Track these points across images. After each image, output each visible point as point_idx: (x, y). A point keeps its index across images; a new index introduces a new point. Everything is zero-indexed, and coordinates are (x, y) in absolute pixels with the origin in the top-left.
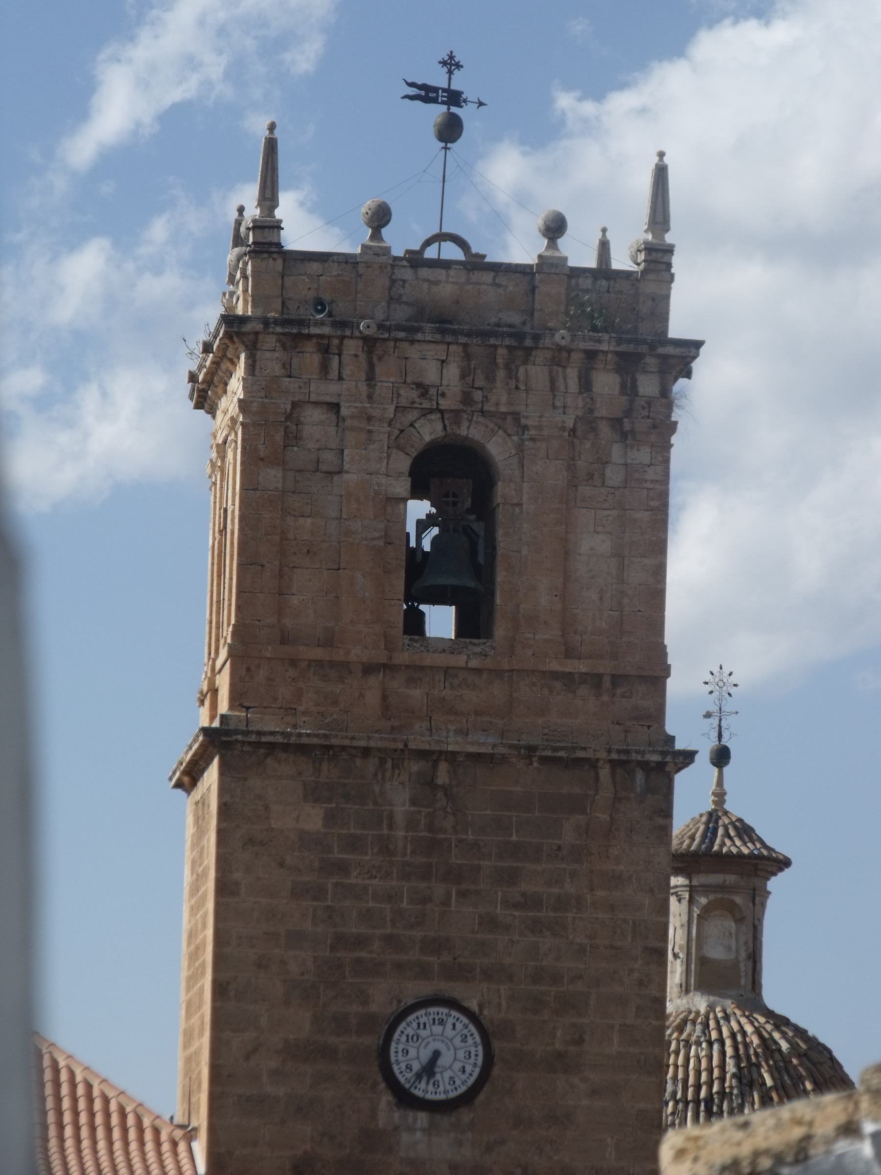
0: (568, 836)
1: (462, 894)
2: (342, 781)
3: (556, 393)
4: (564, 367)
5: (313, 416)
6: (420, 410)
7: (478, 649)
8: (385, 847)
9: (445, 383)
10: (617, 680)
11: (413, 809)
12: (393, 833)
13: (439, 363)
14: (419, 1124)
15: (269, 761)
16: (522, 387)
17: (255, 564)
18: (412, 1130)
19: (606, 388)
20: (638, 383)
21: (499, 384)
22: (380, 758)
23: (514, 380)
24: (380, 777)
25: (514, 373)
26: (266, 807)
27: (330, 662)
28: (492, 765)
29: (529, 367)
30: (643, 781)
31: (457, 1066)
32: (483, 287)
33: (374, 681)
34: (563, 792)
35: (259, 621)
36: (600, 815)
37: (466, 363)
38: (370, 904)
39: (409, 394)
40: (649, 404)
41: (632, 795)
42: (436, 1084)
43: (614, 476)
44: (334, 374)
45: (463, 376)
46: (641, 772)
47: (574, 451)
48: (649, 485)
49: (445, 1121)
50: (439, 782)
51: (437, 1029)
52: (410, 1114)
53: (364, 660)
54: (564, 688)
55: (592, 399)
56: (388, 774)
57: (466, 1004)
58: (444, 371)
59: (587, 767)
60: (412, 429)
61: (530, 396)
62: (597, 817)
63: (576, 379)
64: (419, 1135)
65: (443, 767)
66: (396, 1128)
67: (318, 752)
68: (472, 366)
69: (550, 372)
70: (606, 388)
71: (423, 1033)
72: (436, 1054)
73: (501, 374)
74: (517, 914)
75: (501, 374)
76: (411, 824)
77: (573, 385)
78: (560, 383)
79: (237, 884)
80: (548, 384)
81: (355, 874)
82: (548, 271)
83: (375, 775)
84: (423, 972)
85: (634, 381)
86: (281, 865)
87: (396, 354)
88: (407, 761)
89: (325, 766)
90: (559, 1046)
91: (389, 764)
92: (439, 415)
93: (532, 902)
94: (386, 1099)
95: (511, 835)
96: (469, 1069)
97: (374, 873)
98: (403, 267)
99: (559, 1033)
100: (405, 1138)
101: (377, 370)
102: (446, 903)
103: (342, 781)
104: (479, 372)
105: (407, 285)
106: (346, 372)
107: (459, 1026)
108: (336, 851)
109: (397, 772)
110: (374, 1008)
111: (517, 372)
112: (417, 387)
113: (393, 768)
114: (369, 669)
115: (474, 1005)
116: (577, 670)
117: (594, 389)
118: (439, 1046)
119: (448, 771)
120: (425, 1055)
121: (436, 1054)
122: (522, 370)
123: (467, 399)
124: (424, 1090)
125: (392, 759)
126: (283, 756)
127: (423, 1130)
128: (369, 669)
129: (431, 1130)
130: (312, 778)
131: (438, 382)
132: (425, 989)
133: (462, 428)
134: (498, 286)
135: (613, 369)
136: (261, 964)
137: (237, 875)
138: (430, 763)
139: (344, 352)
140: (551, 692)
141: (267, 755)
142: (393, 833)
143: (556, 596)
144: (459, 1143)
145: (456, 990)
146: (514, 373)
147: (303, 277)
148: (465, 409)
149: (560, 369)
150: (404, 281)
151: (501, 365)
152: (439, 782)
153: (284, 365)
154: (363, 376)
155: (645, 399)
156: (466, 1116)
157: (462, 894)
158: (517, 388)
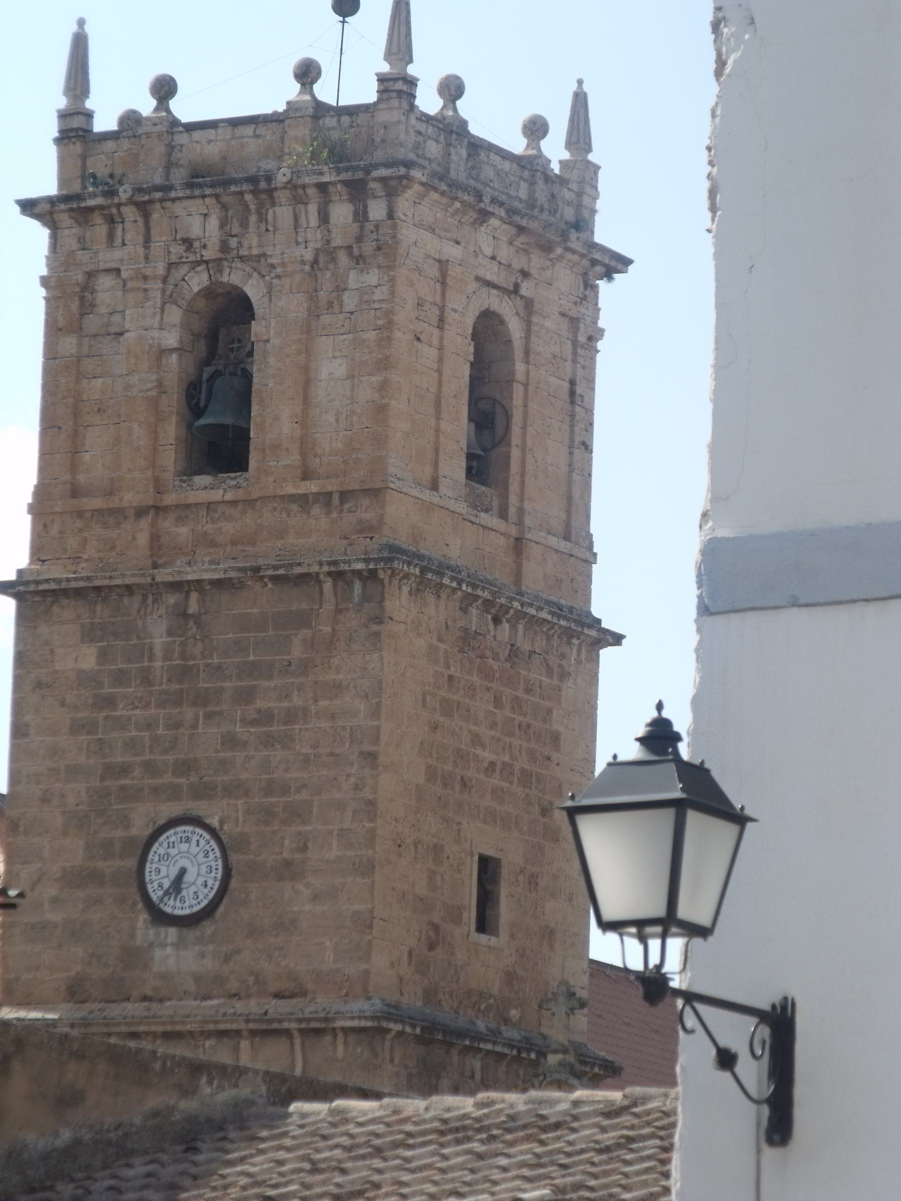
0: (297, 651)
1: (209, 716)
2: (112, 620)
3: (298, 230)
4: (306, 204)
5: (105, 282)
6: (189, 264)
8: (146, 678)
9: (207, 235)
10: (345, 495)
11: (169, 639)
12: (152, 664)
13: (202, 218)
14: (169, 940)
15: (55, 609)
16: (271, 229)
17: (54, 427)
18: (163, 945)
19: (342, 219)
20: (369, 209)
21: (252, 229)
22: (143, 594)
23: (264, 223)
24: (142, 612)
25: (264, 217)
26: (52, 652)
27: (110, 509)
28: (233, 590)
29: (277, 209)
30: (360, 590)
31: (201, 880)
32: (246, 140)
33: (145, 523)
34: (293, 609)
35: (55, 479)
36: (323, 628)
37: (224, 213)
38: (133, 734)
39: (177, 250)
40: (377, 227)
41: (351, 605)
42: (183, 900)
43: (350, 301)
44: (118, 242)
45: (222, 226)
46: (358, 582)
47: (317, 282)
48: (376, 306)
49: (191, 934)
50: (190, 611)
51: (184, 847)
52: (162, 930)
53: (134, 504)
54: (300, 509)
55: (329, 231)
56: (150, 609)
57: (208, 821)
58: (206, 223)
59: (313, 583)
60: (182, 283)
61: (276, 236)
62: (321, 630)
63: (316, 214)
64: (169, 950)
65: (194, 596)
66: (151, 945)
67: (93, 596)
68: (230, 215)
69: (294, 210)
70: (342, 219)
71: (173, 852)
72: (183, 872)
73: (253, 219)
74: (253, 730)
75: (253, 219)
76: (167, 655)
77: (314, 220)
78: (303, 221)
79: (27, 726)
80: (292, 222)
81: (121, 706)
82: (294, 116)
83: (139, 611)
84: (174, 793)
85: (365, 207)
86: (63, 704)
87: (168, 215)
88: (164, 595)
89: (99, 608)
90: (286, 855)
91: (150, 600)
92: (204, 266)
93: (266, 718)
94: (143, 916)
95: (249, 655)
96: (210, 882)
97: (137, 703)
98: (181, 132)
99: (287, 842)
100: (158, 953)
101: (152, 232)
102: (195, 726)
103: (112, 620)
104: (235, 220)
105: (184, 149)
106: (128, 237)
107: (202, 842)
108: (106, 686)
109: (156, 606)
110: (134, 832)
111: (267, 215)
112: (183, 242)
113: (154, 602)
114: (140, 512)
115: (215, 822)
116: (309, 492)
117: (331, 221)
118: (184, 863)
119: (198, 601)
120: (174, 872)
121: (183, 872)
122: (270, 212)
123: (224, 247)
124: (172, 907)
125: (153, 594)
126: (65, 602)
127: (173, 945)
128: (140, 512)
129: (180, 944)
130: (89, 620)
131: (201, 235)
132: (174, 809)
133: (224, 275)
134: (258, 137)
135: (348, 199)
136: (45, 799)
137: (28, 718)
138: (183, 594)
139: (126, 220)
140: (289, 515)
141: (53, 603)
142: (152, 664)
143: (296, 422)
144: (202, 955)
145: (200, 808)
146: (264, 217)
147: (101, 156)
148: (223, 256)
149: (302, 207)
150: (182, 146)
151: (253, 211)
152: (190, 611)
153: (79, 239)
154: (141, 239)
155: (373, 223)
156: (208, 928)
157: (209, 716)
158: (267, 230)
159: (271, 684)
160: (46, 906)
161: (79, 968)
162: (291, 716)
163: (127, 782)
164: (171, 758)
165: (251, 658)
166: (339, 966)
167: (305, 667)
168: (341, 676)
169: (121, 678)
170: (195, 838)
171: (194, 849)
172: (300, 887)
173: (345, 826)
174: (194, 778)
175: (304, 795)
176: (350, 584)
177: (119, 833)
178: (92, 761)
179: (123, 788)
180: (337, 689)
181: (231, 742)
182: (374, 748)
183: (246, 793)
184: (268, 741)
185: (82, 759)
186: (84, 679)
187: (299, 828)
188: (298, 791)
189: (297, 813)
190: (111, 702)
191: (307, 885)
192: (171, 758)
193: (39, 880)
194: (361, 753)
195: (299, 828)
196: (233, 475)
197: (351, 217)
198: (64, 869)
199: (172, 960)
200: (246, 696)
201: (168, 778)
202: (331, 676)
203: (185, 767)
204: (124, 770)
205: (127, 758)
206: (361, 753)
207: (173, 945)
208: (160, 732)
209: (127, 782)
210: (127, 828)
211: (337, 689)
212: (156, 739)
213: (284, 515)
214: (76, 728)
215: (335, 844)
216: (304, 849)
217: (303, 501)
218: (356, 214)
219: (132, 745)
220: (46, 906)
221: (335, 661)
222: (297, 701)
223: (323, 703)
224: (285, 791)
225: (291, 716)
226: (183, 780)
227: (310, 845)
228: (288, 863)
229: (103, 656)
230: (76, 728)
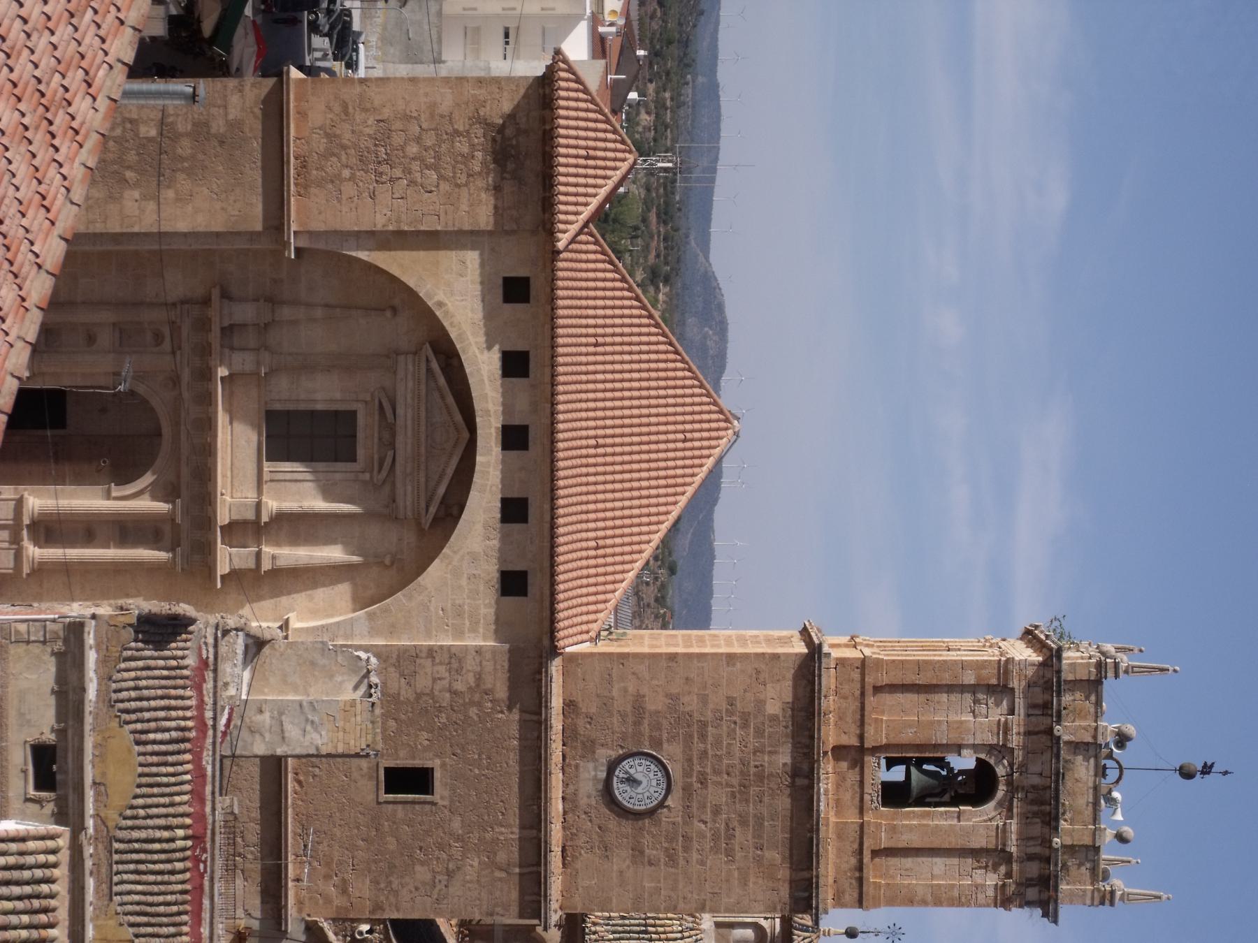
1: (733, 795)
7: (875, 798)
18: (595, 769)
45: (1034, 787)
52: (605, 768)
64: (593, 773)
66: (597, 760)
71: (651, 775)
73: (1035, 808)
78: (1031, 843)
84: (687, 774)
90: (647, 851)
100: (591, 765)
107: (656, 795)
115: (669, 802)
120: (638, 777)
121: (638, 783)
122: (1038, 820)
127: (596, 776)
144: (589, 797)
145: (677, 792)
159: (750, 837)
160: (622, 685)
161: (584, 710)
162: (729, 853)
163: (696, 740)
164: (709, 770)
165: (766, 823)
166: (580, 889)
167: (759, 861)
168: (751, 885)
169: (759, 733)
170: (660, 790)
171: (652, 790)
172: (628, 862)
173: (662, 892)
174: (697, 785)
175: (682, 862)
176: (805, 890)
177: (665, 736)
178: (709, 713)
179: (691, 736)
180: (744, 883)
181: (716, 811)
182: (708, 908)
183: (685, 823)
184: (716, 837)
185: (711, 706)
186: (760, 704)
187: (662, 860)
188: (684, 858)
189: (672, 859)
190: (745, 725)
191: (628, 867)
192: (709, 770)
193: (638, 678)
194: (705, 900)
195: (662, 860)
196: (880, 799)
197: (1029, 876)
198: (644, 696)
199: (587, 775)
200: (744, 822)
201: (697, 768)
202: (752, 879)
203: (703, 782)
204: (703, 737)
205: (710, 739)
206: (705, 900)
207: (596, 776)
208: (725, 761)
209: (696, 740)
210: (668, 741)
211: (744, 883)
212: (719, 758)
213: (852, 839)
214: (731, 701)
215: (653, 885)
216: (650, 864)
217: (860, 851)
218: (1031, 879)
219: (718, 743)
220: (622, 685)
221: (760, 881)
222: (739, 855)
223: (736, 874)
224: (686, 849)
225: (729, 853)
226: (695, 779)
227: (653, 868)
228: (642, 852)
229: (774, 718)
230: (731, 701)
